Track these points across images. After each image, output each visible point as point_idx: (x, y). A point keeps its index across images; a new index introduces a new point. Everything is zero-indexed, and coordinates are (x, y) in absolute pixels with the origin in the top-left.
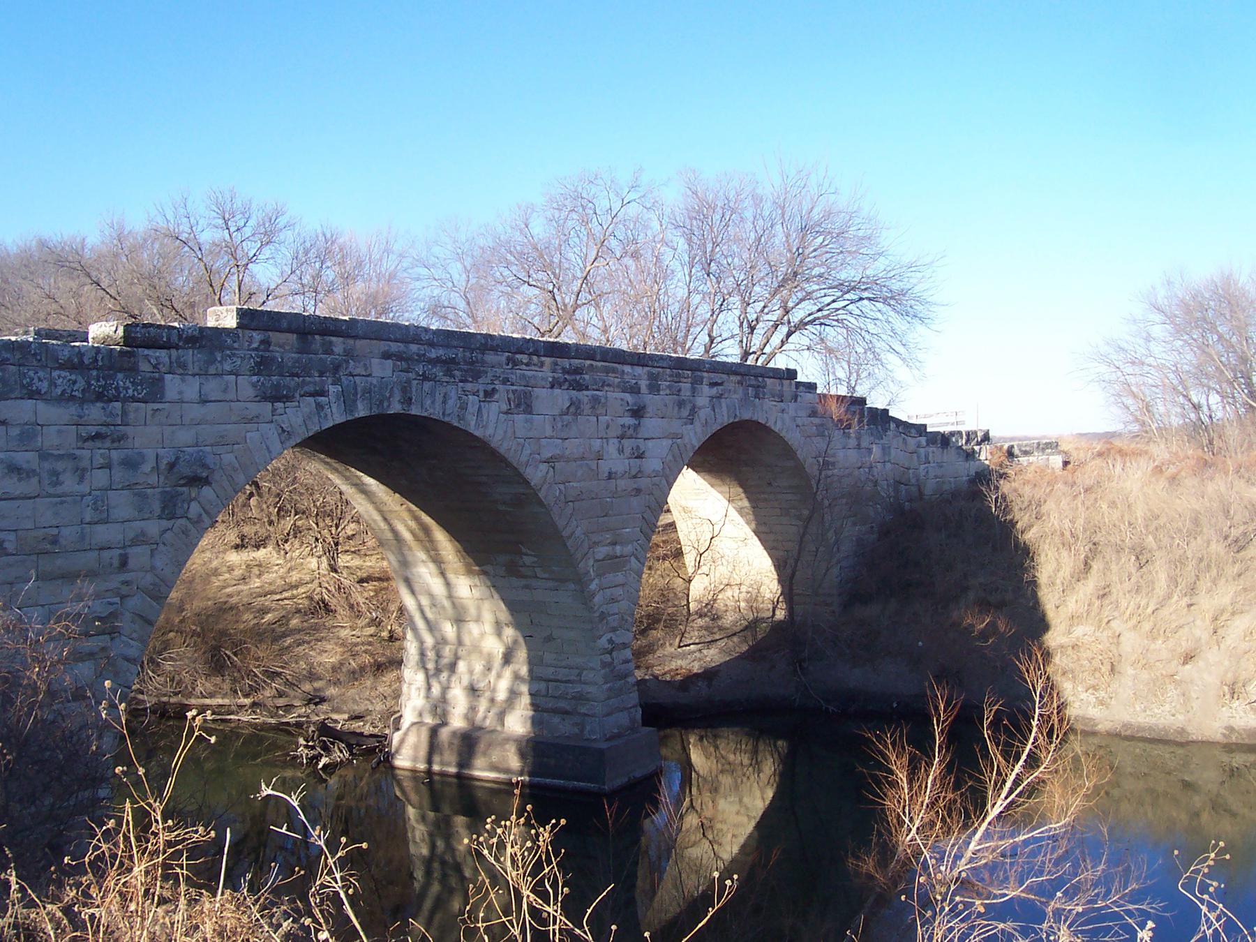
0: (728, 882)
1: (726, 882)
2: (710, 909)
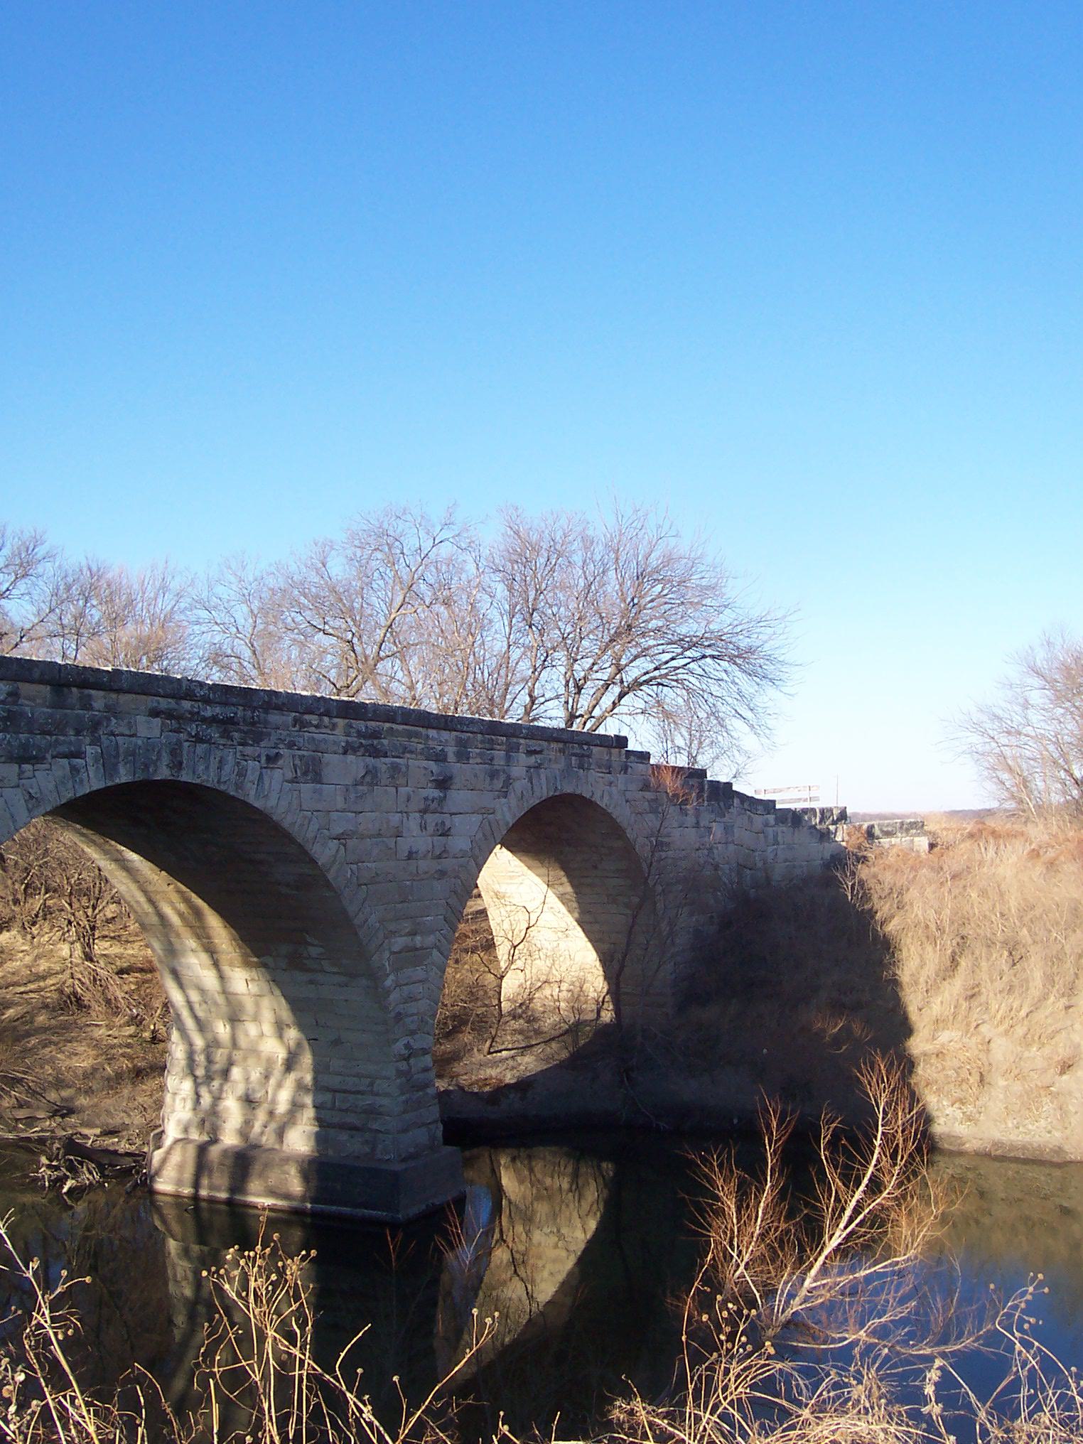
0: (489, 1321)
1: (486, 1321)
2: (468, 1350)
